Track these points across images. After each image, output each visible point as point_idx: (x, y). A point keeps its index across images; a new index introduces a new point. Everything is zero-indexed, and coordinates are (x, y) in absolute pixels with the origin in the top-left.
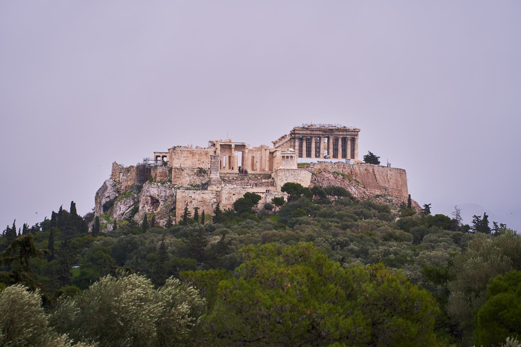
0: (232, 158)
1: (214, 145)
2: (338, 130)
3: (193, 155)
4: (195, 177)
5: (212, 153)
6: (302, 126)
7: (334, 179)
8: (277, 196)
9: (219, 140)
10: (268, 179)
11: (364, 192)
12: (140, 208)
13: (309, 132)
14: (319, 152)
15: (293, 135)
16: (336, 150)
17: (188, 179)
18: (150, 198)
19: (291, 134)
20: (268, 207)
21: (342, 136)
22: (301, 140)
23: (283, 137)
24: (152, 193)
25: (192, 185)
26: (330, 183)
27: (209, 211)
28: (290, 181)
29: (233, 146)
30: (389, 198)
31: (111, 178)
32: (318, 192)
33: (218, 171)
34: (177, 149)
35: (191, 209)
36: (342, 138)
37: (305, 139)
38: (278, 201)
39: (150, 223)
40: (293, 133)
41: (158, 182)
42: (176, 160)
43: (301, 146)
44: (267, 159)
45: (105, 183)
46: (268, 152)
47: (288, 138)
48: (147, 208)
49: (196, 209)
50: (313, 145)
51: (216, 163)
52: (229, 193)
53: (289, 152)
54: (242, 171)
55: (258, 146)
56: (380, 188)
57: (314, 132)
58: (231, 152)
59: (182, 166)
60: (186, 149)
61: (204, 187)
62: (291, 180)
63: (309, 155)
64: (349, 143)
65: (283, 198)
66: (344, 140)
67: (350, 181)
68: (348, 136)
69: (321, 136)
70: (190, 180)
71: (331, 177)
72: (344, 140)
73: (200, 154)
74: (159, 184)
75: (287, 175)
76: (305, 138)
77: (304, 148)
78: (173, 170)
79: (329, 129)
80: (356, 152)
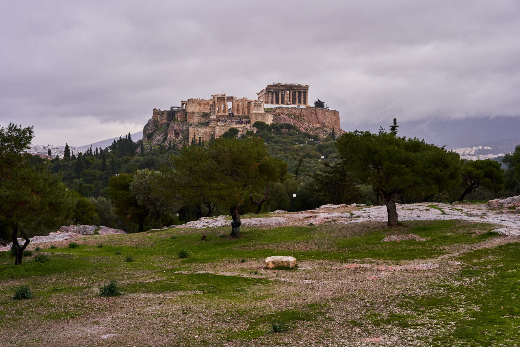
2: (296, 86)
4: (202, 118)
5: (211, 103)
7: (288, 118)
16: (294, 99)
17: (197, 119)
19: (266, 89)
20: (243, 136)
22: (272, 92)
23: (262, 91)
24: (175, 128)
25: (199, 123)
27: (207, 139)
28: (259, 121)
29: (226, 98)
30: (325, 129)
32: (276, 127)
37: (275, 92)
38: (250, 133)
39: (172, 148)
43: (272, 97)
46: (247, 102)
47: (264, 92)
48: (173, 137)
49: (200, 138)
50: (280, 96)
54: (232, 115)
56: (319, 123)
61: (207, 124)
62: (260, 120)
64: (302, 94)
65: (253, 131)
66: (300, 93)
72: (300, 93)
77: (274, 98)
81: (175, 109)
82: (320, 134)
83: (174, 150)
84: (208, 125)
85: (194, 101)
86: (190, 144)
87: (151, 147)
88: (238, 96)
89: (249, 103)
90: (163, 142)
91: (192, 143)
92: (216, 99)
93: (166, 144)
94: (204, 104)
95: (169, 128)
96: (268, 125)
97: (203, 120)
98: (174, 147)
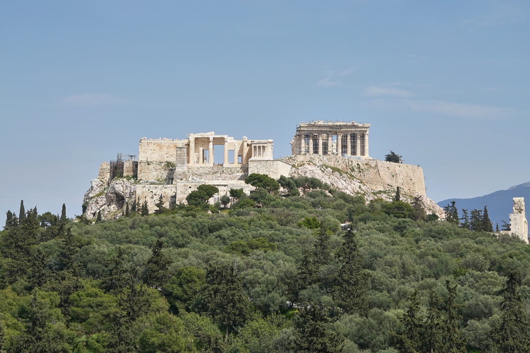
3: (160, 148)
7: (320, 172)
11: (360, 187)
16: (344, 147)
17: (155, 173)
18: (115, 195)
20: (225, 200)
29: (211, 139)
41: (125, 177)
51: (182, 155)
52: (185, 186)
59: (149, 160)
65: (241, 190)
66: (354, 137)
67: (341, 175)
68: (357, 132)
70: (157, 175)
75: (259, 167)
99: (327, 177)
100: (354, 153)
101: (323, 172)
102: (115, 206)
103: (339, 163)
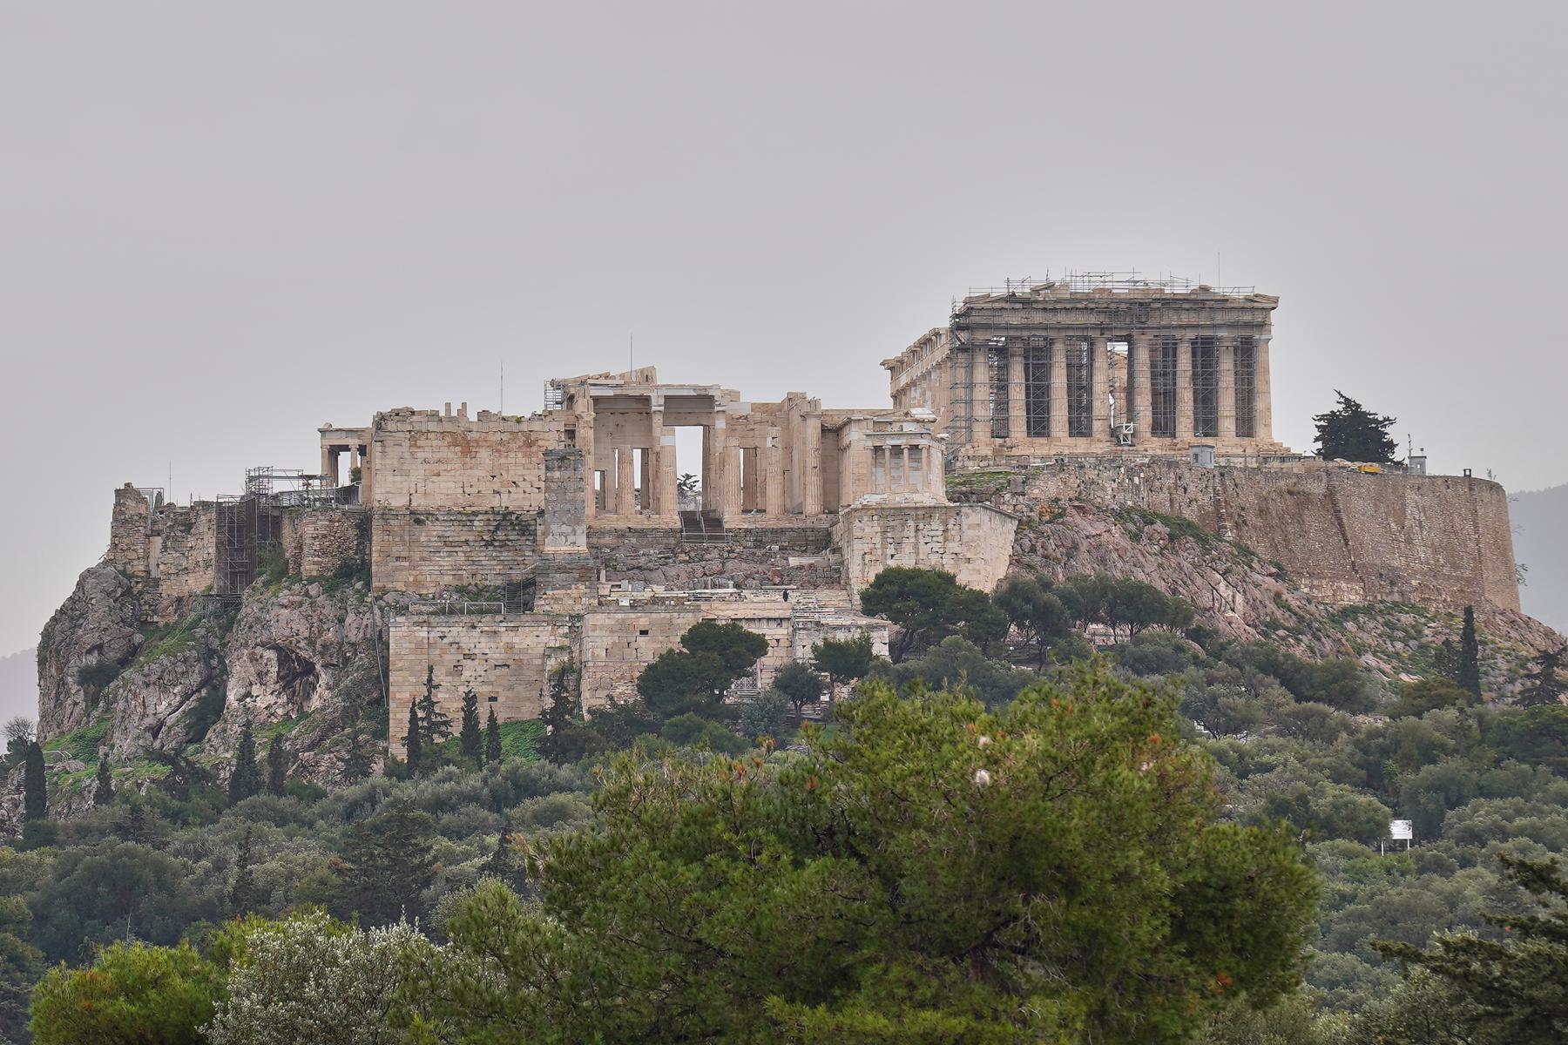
0: (652, 457)
1: (571, 398)
6: (1001, 291)
7: (1125, 543)
8: (841, 637)
9: (593, 370)
10: (817, 552)
11: (1278, 595)
12: (232, 697)
13: (1038, 318)
14: (1089, 408)
15: (963, 336)
16: (1164, 399)
18: (270, 655)
21: (1191, 334)
26: (1103, 561)
28: (906, 561)
29: (657, 404)
31: (106, 563)
33: (579, 522)
34: (391, 426)
35: (449, 703)
36: (1193, 343)
40: (966, 319)
41: (311, 580)
42: (390, 478)
43: (1001, 387)
44: (812, 460)
45: (80, 585)
46: (812, 429)
47: (941, 351)
48: (265, 699)
50: (1059, 379)
51: (572, 486)
53: (909, 427)
55: (777, 397)
56: (1356, 571)
57: (1063, 319)
58: (649, 429)
59: (419, 503)
60: (433, 426)
61: (518, 597)
63: (1038, 425)
66: (1205, 351)
68: (1222, 333)
69: (1095, 334)
71: (1116, 535)
72: (1205, 351)
73: (498, 448)
74: (314, 589)
76: (1018, 347)
77: (1017, 395)
78: (376, 524)
79: (1132, 302)
80: (1259, 405)
81: (277, 487)
82: (1369, 659)
83: (279, 790)
84: (528, 607)
85: (417, 423)
86: (400, 752)
87: (104, 775)
88: (753, 385)
89: (833, 432)
90: (196, 734)
91: (412, 740)
92: (583, 407)
93: (218, 752)
94: (498, 448)
95: (239, 634)
96: (980, 596)
97: (492, 570)
98: (278, 774)
99: (1151, 564)
100: (1207, 424)
101: (1135, 537)
102: (271, 699)
103: (1191, 495)
